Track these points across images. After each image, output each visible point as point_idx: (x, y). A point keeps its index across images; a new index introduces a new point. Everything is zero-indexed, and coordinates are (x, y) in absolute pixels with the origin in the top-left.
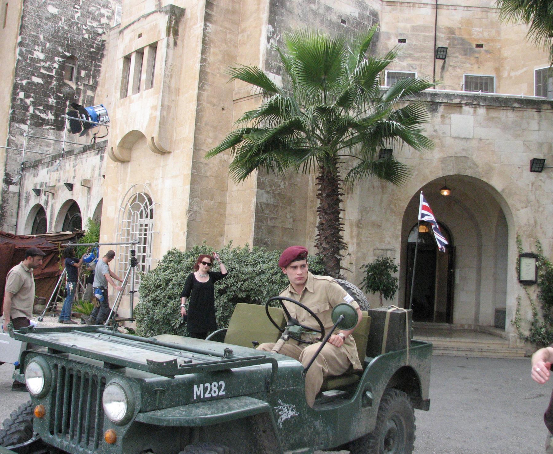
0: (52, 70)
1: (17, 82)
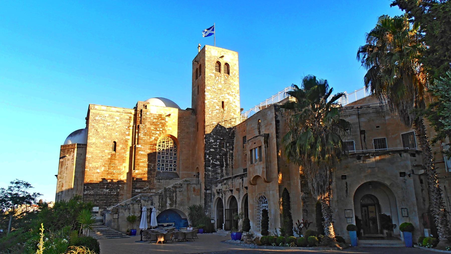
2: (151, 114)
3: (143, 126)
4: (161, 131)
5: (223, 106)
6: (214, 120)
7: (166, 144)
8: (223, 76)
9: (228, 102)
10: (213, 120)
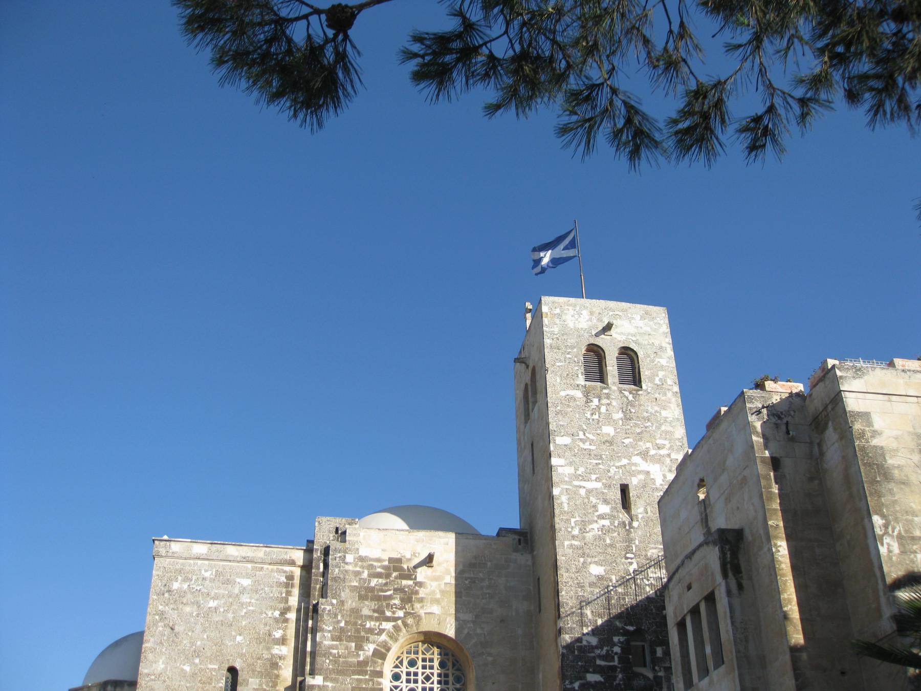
0: (613, 657)
1: (566, 688)
2: (362, 559)
3: (332, 605)
4: (399, 618)
5: (626, 503)
6: (593, 560)
7: (420, 671)
8: (617, 393)
9: (644, 487)
10: (589, 560)
